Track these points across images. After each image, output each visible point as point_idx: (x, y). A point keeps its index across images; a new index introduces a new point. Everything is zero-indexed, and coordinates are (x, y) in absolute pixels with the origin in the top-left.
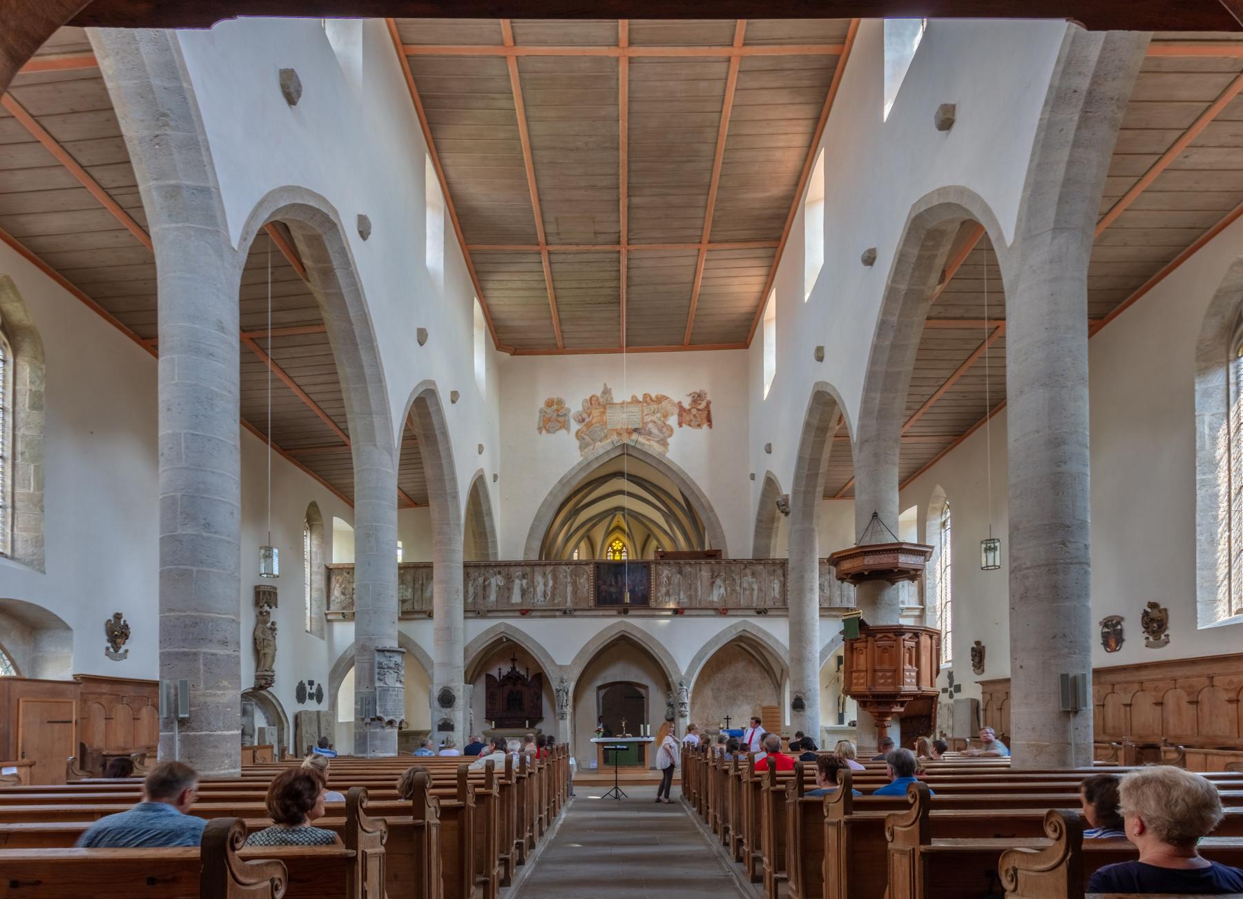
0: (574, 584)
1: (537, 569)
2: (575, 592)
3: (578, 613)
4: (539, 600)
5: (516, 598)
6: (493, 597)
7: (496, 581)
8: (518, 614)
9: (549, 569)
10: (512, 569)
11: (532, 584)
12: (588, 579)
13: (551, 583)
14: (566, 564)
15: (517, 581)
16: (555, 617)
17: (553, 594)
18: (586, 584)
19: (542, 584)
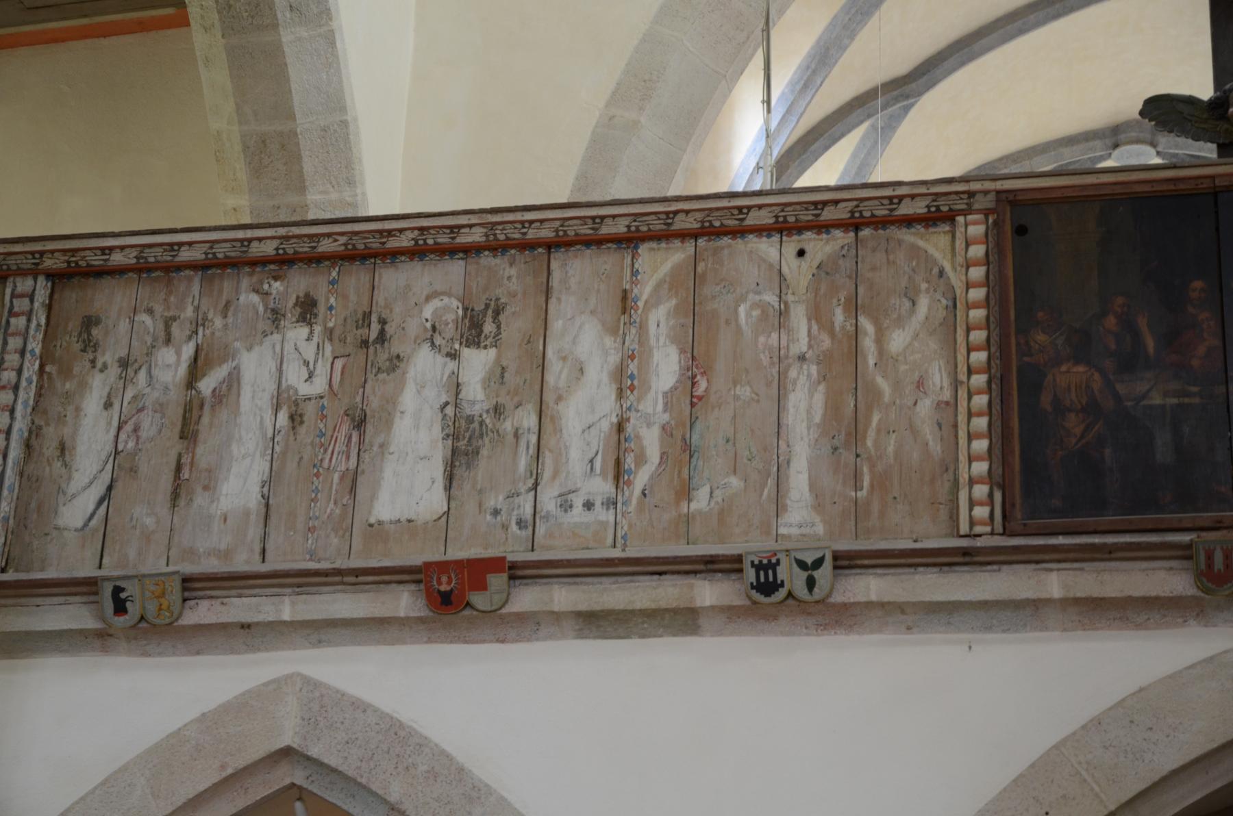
0: (844, 365)
1: (576, 272)
2: (846, 432)
3: (868, 587)
4: (576, 503)
5: (407, 487)
6: (240, 483)
7: (278, 364)
8: (405, 602)
9: (658, 264)
10: (392, 278)
11: (532, 382)
12: (949, 326)
13: (666, 367)
14: (782, 228)
15: (425, 365)
16: (685, 620)
17: (683, 450)
18: (928, 356)
19: (596, 364)
